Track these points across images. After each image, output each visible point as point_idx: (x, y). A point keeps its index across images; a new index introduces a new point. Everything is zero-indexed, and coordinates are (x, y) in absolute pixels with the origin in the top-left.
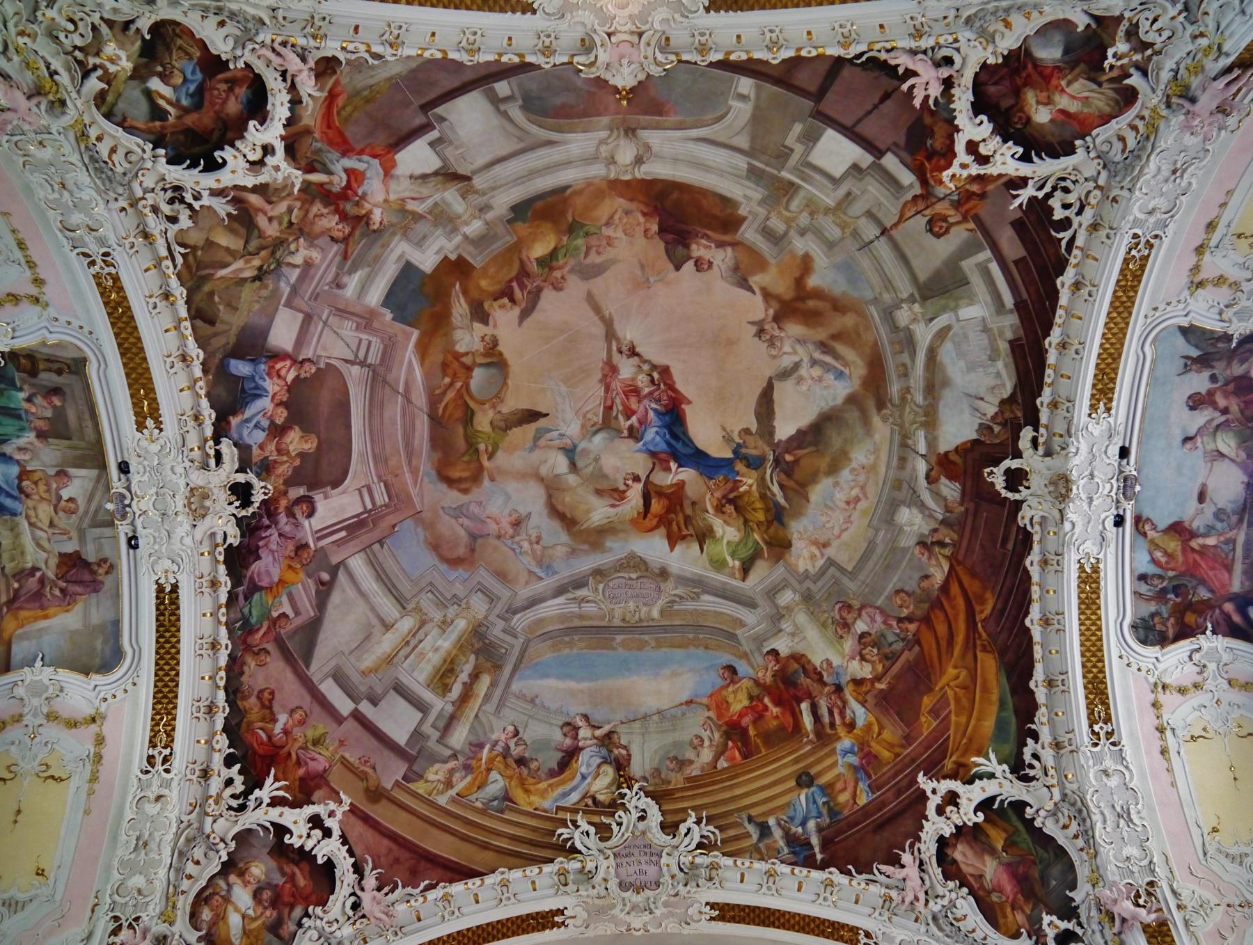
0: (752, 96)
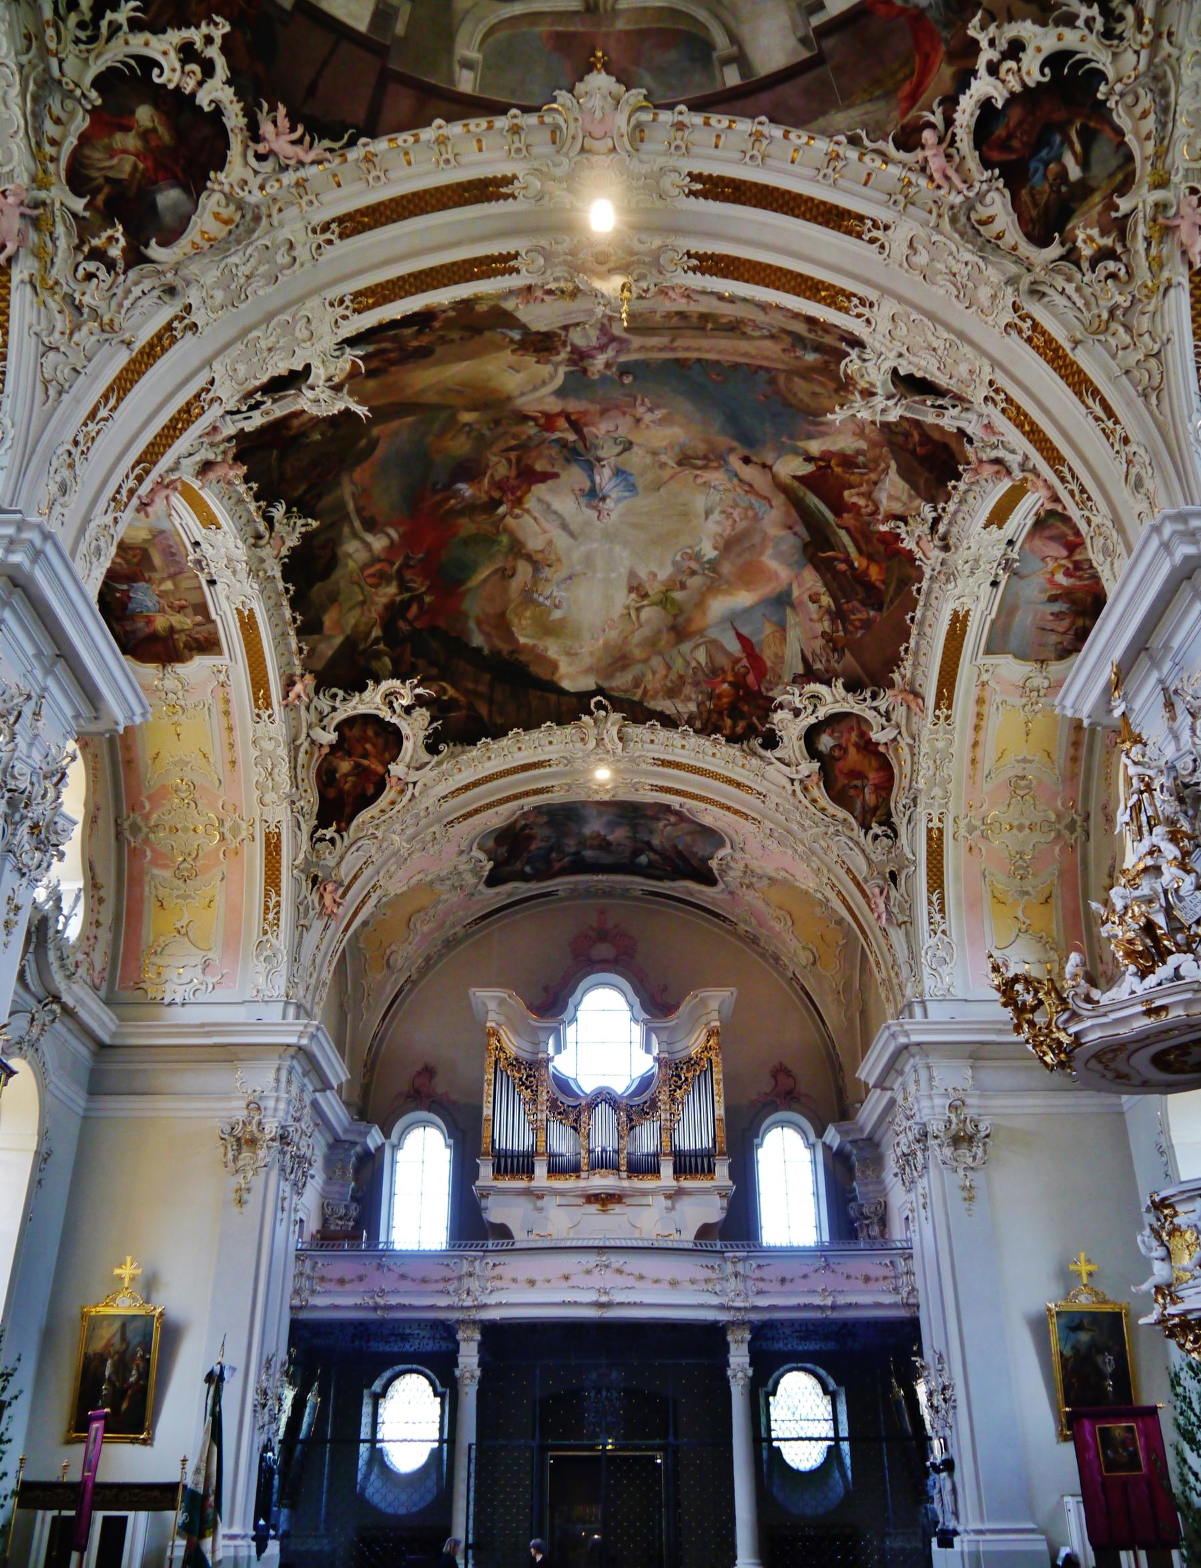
0: (457, 67)
